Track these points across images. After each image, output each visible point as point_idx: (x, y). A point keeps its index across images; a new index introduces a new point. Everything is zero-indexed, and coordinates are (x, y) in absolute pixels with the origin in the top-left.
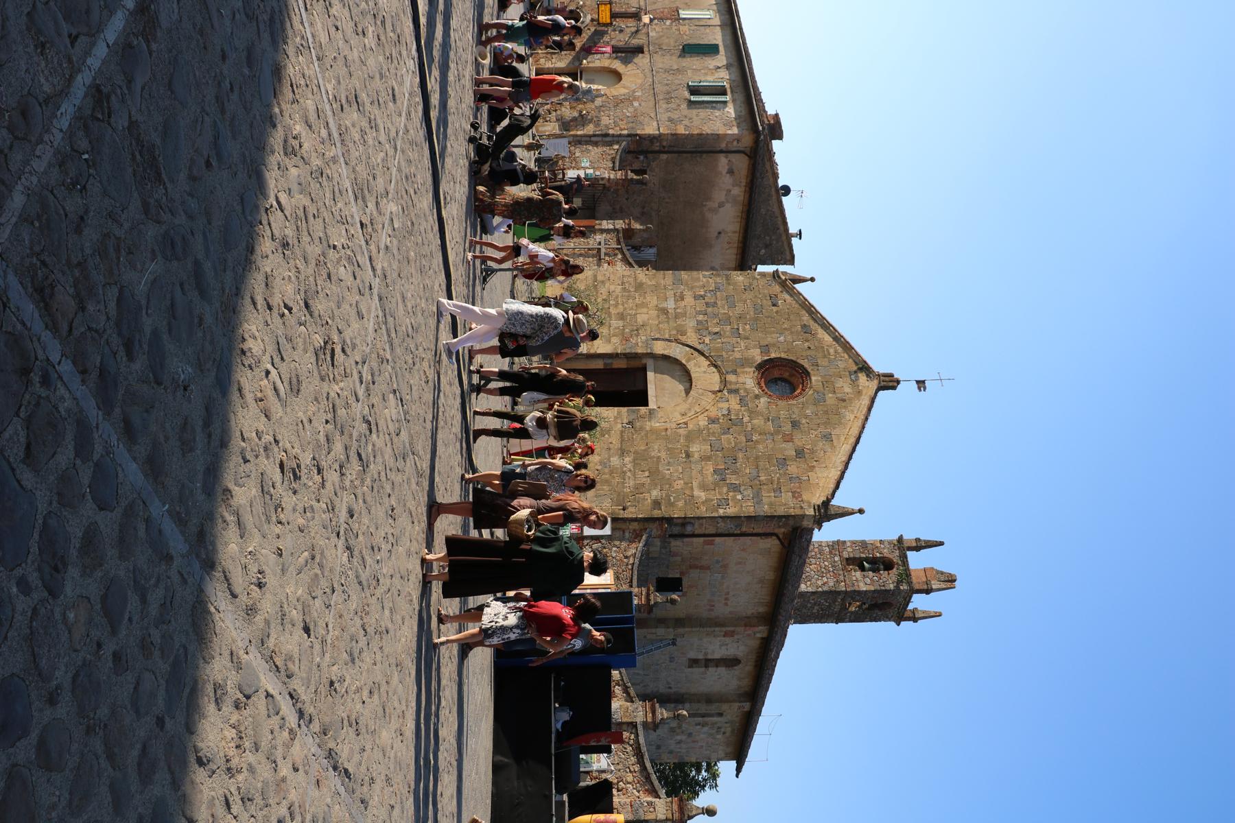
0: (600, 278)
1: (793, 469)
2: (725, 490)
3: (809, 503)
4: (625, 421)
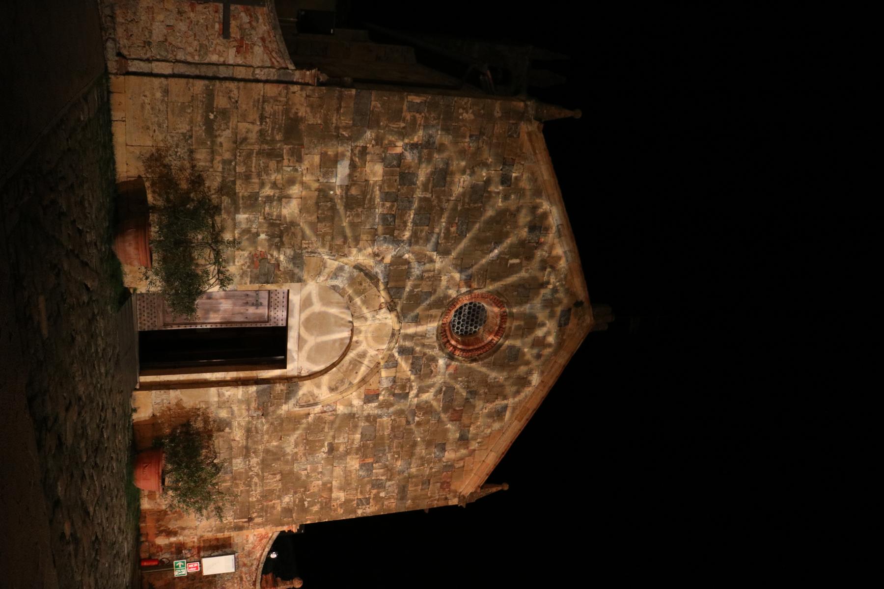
0: (221, 102)
1: (449, 455)
2: (368, 487)
3: (455, 492)
4: (253, 405)
